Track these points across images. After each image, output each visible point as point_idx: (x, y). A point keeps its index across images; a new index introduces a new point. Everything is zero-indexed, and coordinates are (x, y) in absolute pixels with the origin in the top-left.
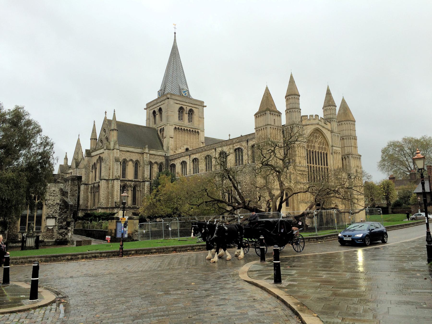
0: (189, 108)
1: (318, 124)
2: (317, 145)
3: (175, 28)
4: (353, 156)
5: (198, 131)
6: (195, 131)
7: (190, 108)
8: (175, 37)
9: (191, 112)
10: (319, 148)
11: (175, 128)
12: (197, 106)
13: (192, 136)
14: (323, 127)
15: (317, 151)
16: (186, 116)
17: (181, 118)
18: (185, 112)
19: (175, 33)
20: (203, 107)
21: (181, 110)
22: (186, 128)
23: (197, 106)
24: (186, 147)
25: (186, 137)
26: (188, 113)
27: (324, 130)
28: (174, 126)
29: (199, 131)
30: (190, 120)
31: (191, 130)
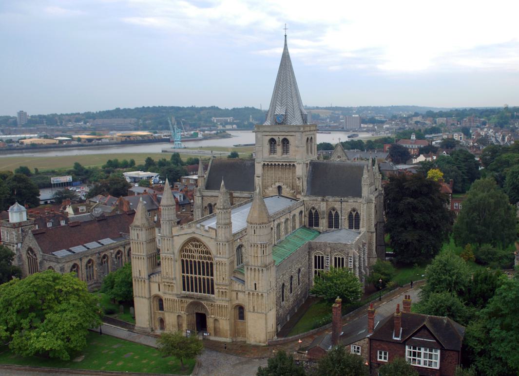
0: (281, 138)
2: (196, 255)
4: (249, 268)
5: (294, 165)
8: (286, 41)
9: (285, 142)
10: (201, 257)
11: (264, 164)
12: (293, 134)
13: (287, 171)
15: (197, 260)
16: (279, 149)
17: (272, 151)
18: (277, 144)
20: (301, 133)
21: (272, 141)
22: (277, 164)
24: (277, 184)
25: (279, 173)
26: (281, 144)
27: (203, 239)
28: (263, 163)
29: (295, 164)
30: (286, 150)
31: (284, 164)
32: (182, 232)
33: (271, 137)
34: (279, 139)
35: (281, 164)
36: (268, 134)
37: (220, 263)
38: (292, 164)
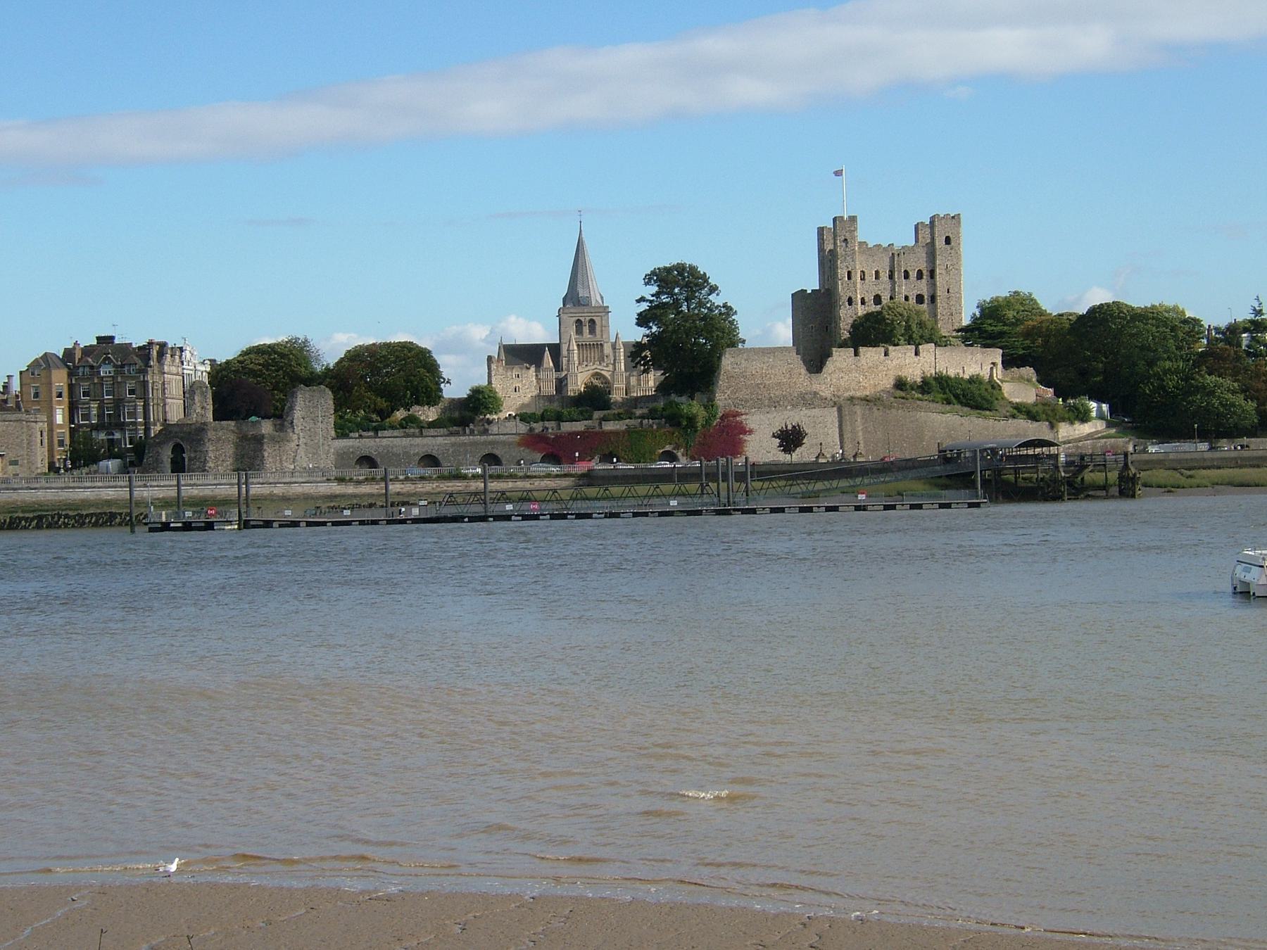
0: (588, 319)
6: (597, 344)
7: (590, 318)
9: (592, 322)
14: (602, 370)
16: (586, 330)
17: (579, 331)
18: (584, 324)
19: (581, 222)
21: (579, 322)
22: (584, 343)
23: (597, 314)
27: (603, 372)
30: (592, 331)
31: (591, 343)
32: (587, 369)
33: (577, 318)
34: (585, 319)
35: (588, 343)
36: (575, 315)
37: (619, 389)
38: (599, 343)
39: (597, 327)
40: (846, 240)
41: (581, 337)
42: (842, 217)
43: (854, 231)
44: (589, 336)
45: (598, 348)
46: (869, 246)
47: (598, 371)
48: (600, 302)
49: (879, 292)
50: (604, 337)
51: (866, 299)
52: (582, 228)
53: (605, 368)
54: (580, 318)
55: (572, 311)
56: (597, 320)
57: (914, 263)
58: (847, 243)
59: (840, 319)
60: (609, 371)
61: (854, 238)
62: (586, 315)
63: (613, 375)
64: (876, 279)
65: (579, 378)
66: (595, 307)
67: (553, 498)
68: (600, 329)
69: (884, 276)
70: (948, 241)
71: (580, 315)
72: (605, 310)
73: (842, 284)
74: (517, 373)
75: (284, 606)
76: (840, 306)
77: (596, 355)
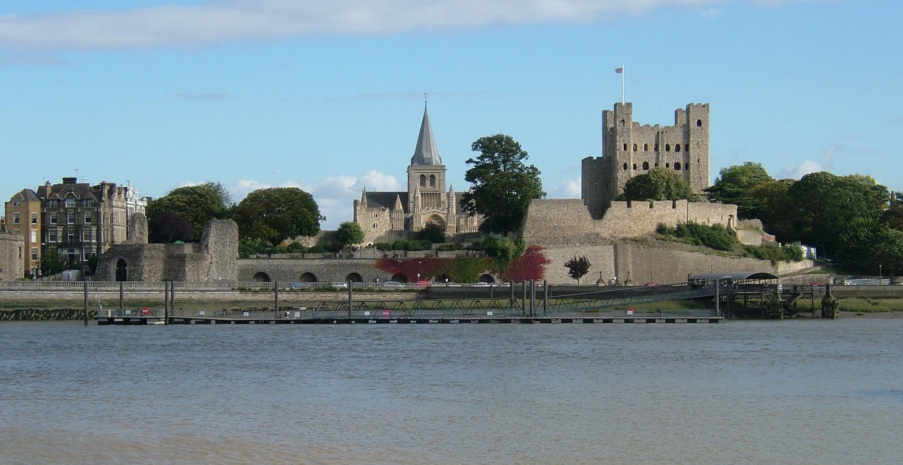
0: (429, 174)
1: (435, 212)
3: (426, 97)
6: (436, 193)
9: (433, 177)
12: (438, 171)
14: (439, 213)
16: (428, 182)
17: (423, 184)
19: (426, 102)
21: (423, 177)
22: (426, 193)
23: (436, 171)
27: (440, 215)
30: (433, 183)
31: (432, 193)
32: (428, 212)
33: (421, 174)
35: (429, 193)
36: (418, 171)
37: (451, 227)
38: (437, 193)
39: (436, 180)
40: (623, 120)
41: (424, 188)
42: (621, 104)
43: (630, 114)
44: (430, 187)
45: (436, 196)
46: (640, 126)
47: (436, 213)
48: (440, 163)
49: (647, 160)
50: (441, 188)
51: (637, 165)
52: (427, 107)
53: (441, 212)
54: (424, 174)
55: (417, 168)
56: (436, 175)
57: (674, 140)
58: (624, 123)
59: (618, 180)
60: (444, 214)
61: (629, 119)
62: (428, 171)
63: (447, 217)
64: (645, 150)
65: (422, 218)
66: (435, 166)
67: (400, 307)
68: (438, 182)
69: (651, 148)
70: (699, 123)
71: (424, 171)
72: (443, 168)
73: (620, 154)
74: (375, 214)
75: (197, 383)
76: (618, 170)
77: (435, 201)
